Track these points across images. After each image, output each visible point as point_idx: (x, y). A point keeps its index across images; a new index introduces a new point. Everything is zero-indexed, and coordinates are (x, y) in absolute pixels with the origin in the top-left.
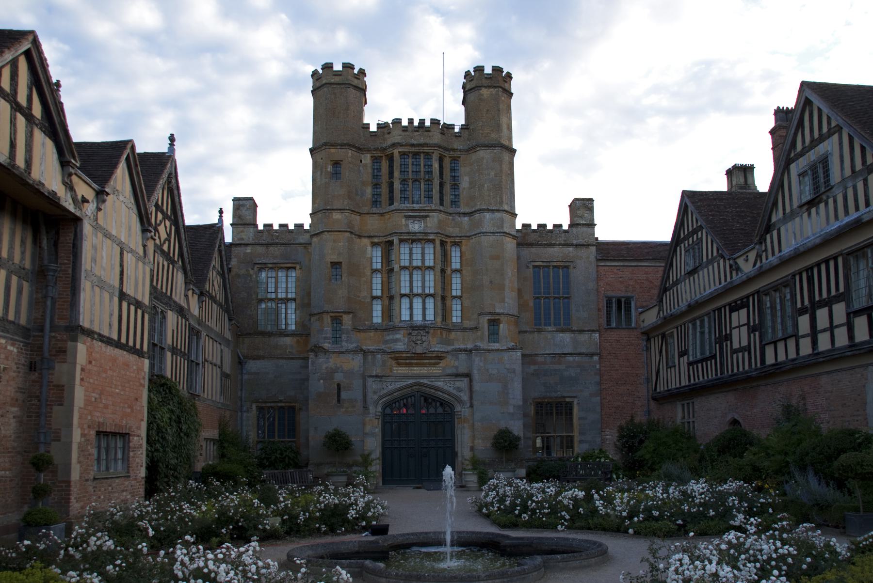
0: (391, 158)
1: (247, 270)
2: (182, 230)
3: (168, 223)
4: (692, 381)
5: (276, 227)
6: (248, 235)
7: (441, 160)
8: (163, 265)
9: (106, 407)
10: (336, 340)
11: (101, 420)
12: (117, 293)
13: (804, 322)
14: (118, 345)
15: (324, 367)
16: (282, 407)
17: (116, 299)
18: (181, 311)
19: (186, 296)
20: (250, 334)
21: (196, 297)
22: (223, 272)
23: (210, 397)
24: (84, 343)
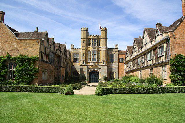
0: (91, 40)
6: (73, 50)
7: (97, 40)
10: (84, 64)
13: (135, 64)
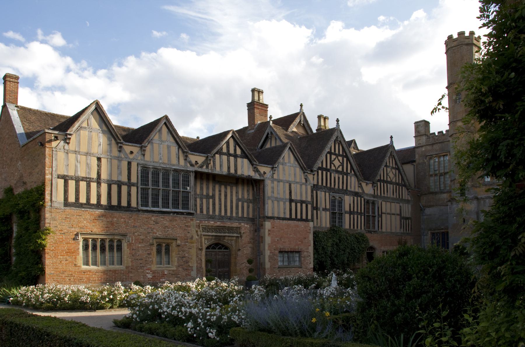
1: (424, 160)
2: (351, 159)
3: (340, 158)
4: (407, 231)
5: (437, 134)
8: (339, 178)
9: (285, 242)
11: (282, 247)
12: (288, 201)
14: (290, 219)
15: (456, 209)
16: (443, 232)
17: (288, 204)
18: (356, 194)
19: (360, 186)
20: (426, 194)
21: (371, 185)
22: (398, 166)
23: (389, 230)
24: (269, 221)
